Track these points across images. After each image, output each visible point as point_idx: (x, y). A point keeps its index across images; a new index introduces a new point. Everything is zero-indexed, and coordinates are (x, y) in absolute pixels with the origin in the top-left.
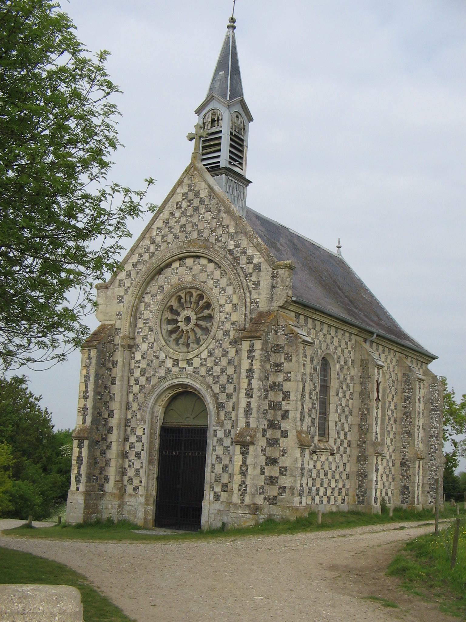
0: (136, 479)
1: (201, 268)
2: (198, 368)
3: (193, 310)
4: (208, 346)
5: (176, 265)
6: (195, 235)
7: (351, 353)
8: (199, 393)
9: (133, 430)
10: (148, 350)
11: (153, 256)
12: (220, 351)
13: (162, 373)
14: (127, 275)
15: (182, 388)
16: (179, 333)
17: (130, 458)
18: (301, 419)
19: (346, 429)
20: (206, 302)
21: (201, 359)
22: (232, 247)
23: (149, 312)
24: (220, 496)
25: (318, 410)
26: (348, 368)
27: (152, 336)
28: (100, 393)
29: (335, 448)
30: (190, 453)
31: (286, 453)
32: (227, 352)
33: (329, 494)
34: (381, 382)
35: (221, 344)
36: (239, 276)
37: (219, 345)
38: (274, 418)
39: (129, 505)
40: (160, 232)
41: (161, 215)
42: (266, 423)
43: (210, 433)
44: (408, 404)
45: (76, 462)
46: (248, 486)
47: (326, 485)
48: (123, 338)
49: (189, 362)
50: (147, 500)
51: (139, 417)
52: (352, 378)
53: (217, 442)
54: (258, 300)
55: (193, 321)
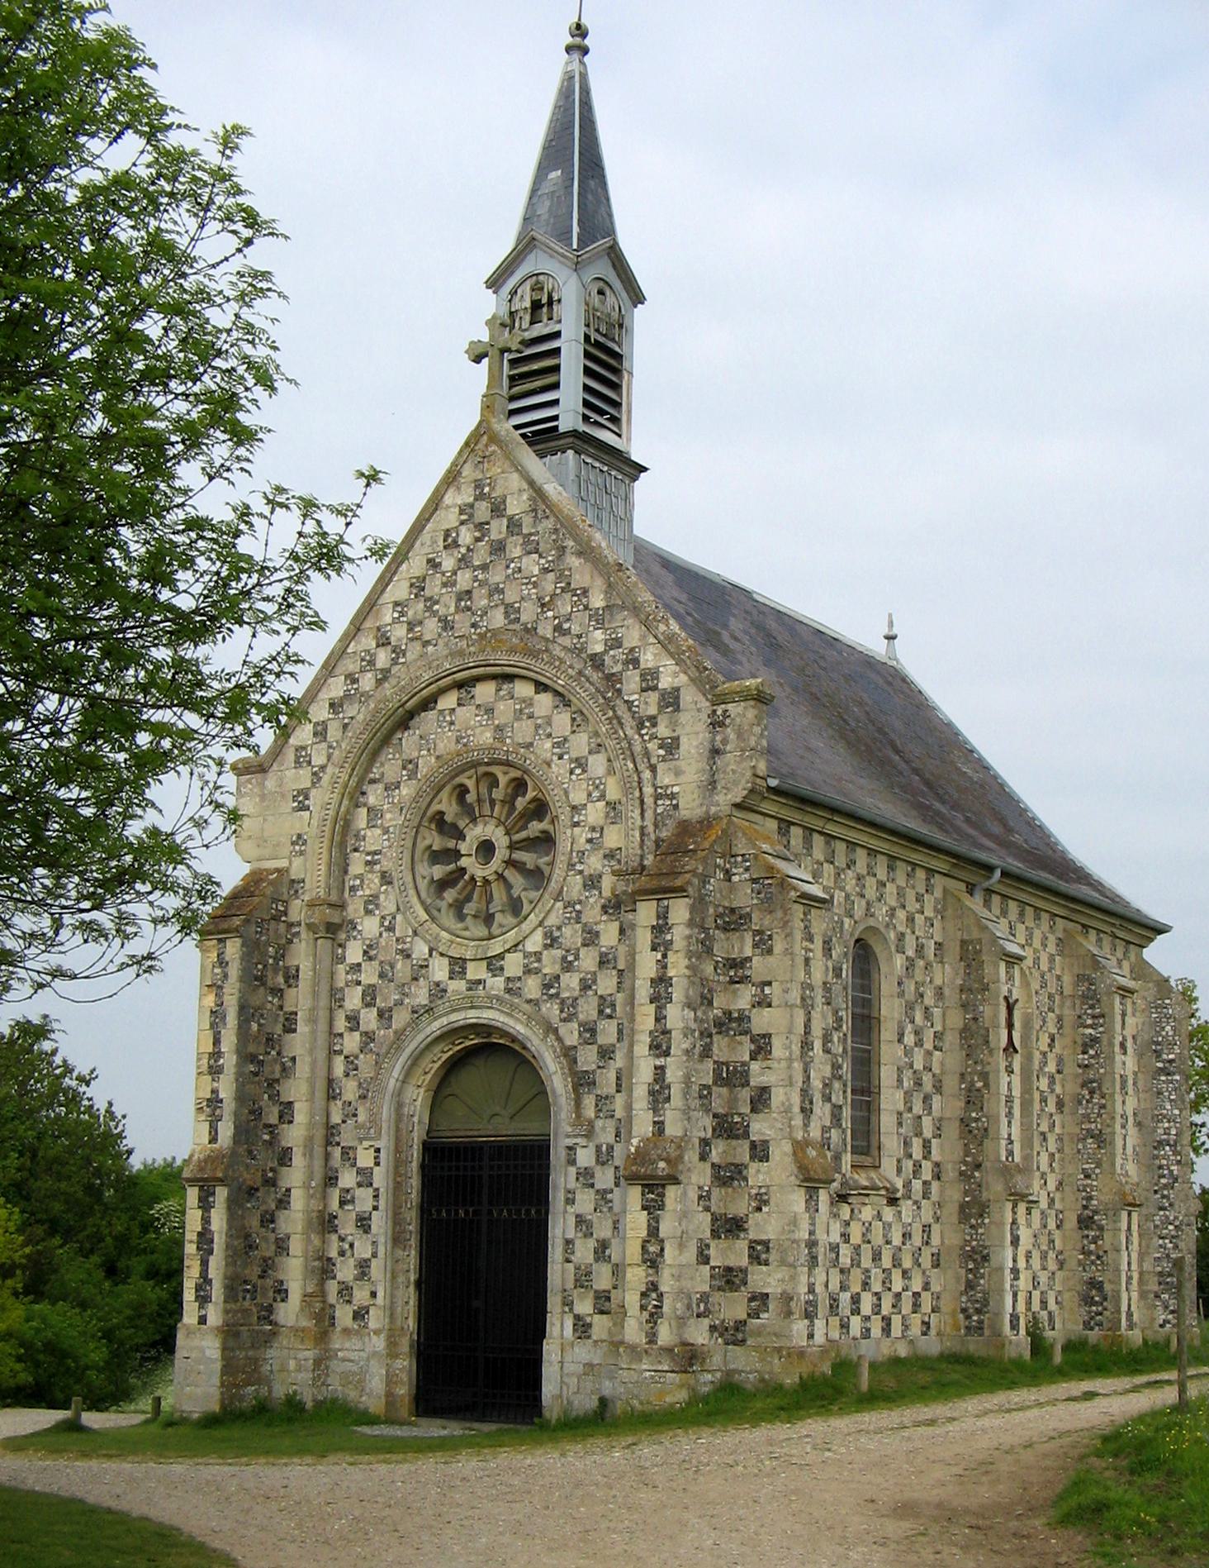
0: (361, 1288)
1: (518, 707)
3: (500, 823)
4: (544, 918)
5: (448, 701)
6: (498, 619)
7: (932, 925)
8: (525, 1048)
9: (348, 1155)
10: (381, 934)
11: (385, 679)
12: (577, 932)
13: (421, 996)
14: (315, 734)
15: (478, 1035)
16: (464, 888)
17: (342, 1232)
18: (803, 1110)
19: (928, 1132)
20: (534, 800)
21: (526, 955)
22: (599, 648)
23: (379, 831)
24: (590, 1325)
25: (849, 1084)
26: (928, 966)
27: (392, 897)
28: (253, 1058)
29: (899, 1184)
30: (505, 1213)
31: (766, 1203)
33: (886, 1309)
34: (1017, 1000)
35: (579, 912)
36: (621, 724)
37: (574, 915)
38: (730, 1108)
39: (344, 1360)
40: (402, 614)
41: (404, 566)
42: (708, 1122)
43: (557, 1155)
44: (1092, 1057)
45: (194, 1246)
46: (665, 1296)
47: (877, 1287)
48: (311, 905)
49: (494, 964)
50: (392, 1343)
51: (361, 1118)
52: (939, 993)
53: (577, 1179)
54: (676, 789)
55: (501, 853)
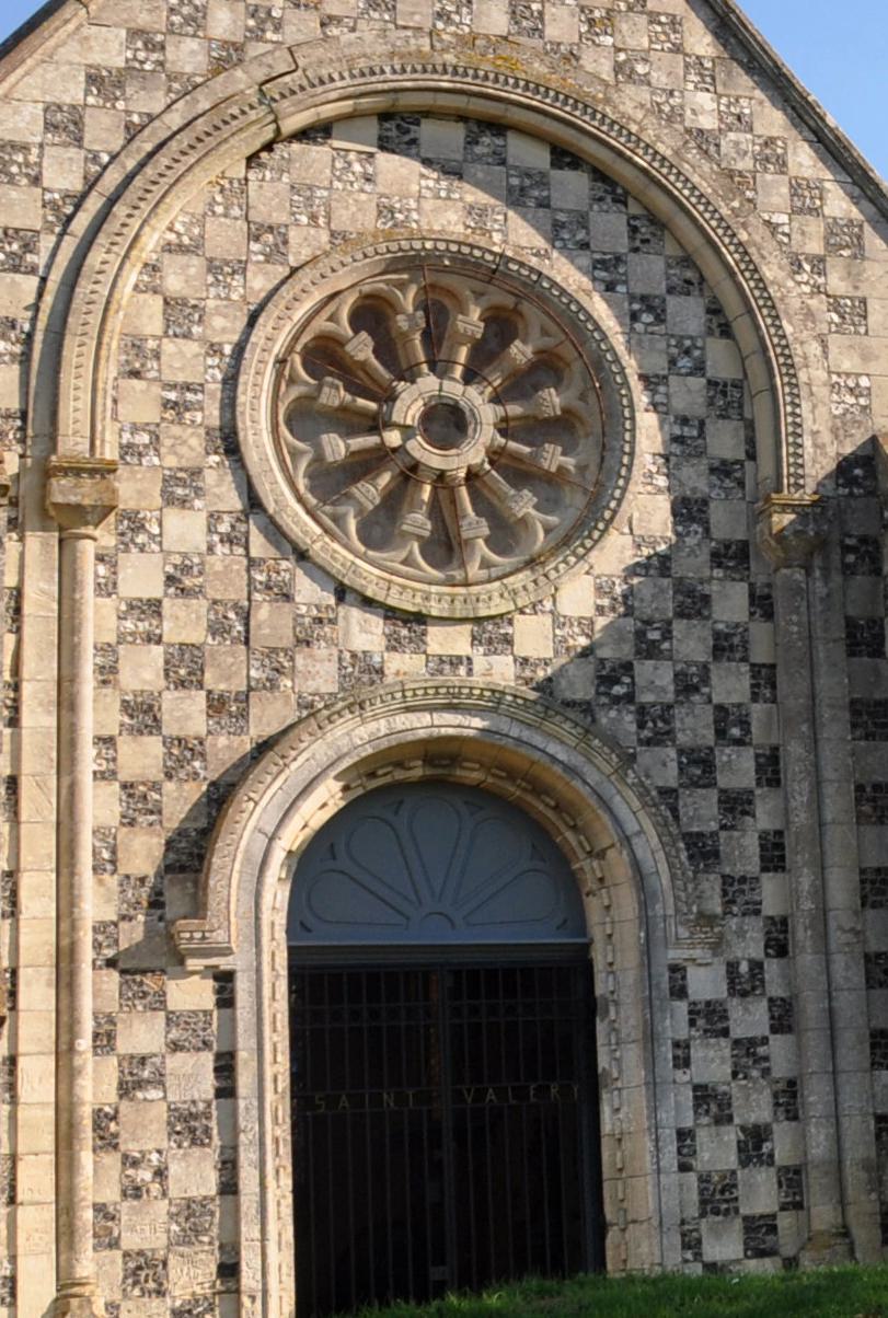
10: (211, 549)
12: (662, 591)
23: (192, 348)
32: (706, 599)
53: (692, 1023)
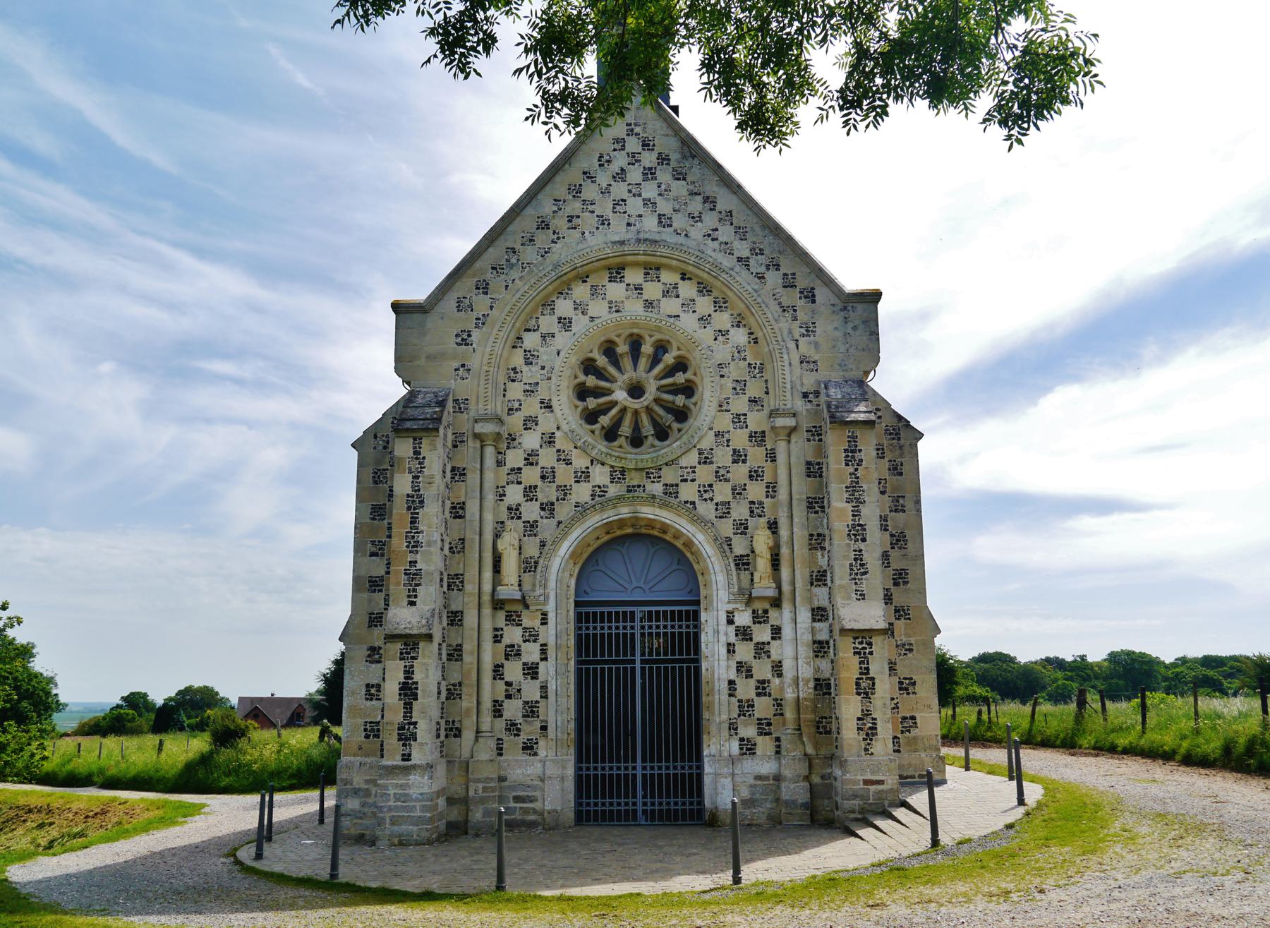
2: (677, 485)
53: (737, 635)
54: (816, 358)
